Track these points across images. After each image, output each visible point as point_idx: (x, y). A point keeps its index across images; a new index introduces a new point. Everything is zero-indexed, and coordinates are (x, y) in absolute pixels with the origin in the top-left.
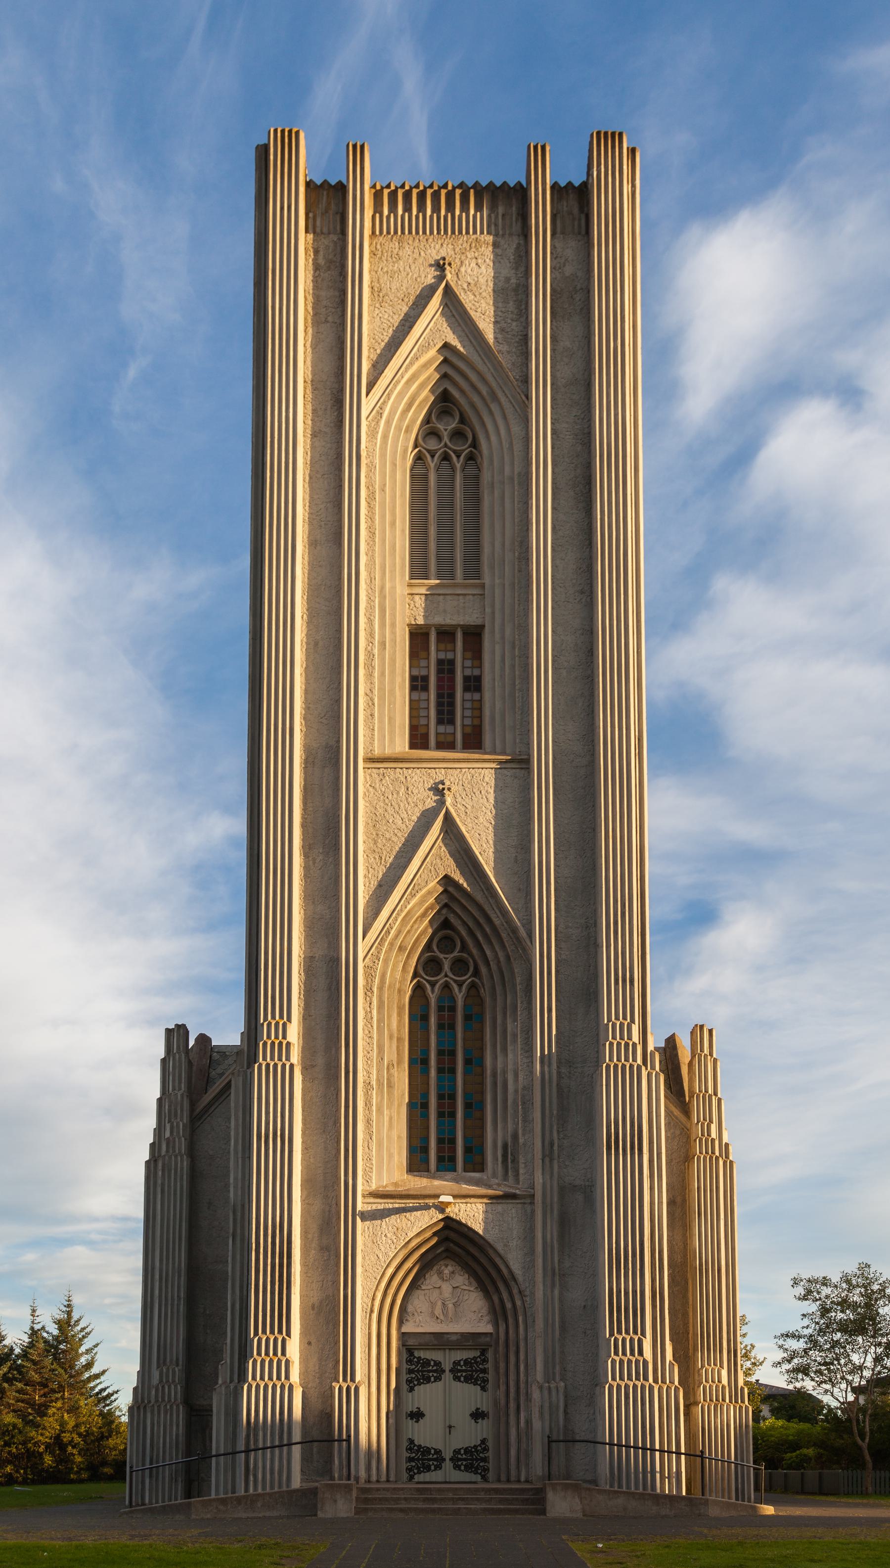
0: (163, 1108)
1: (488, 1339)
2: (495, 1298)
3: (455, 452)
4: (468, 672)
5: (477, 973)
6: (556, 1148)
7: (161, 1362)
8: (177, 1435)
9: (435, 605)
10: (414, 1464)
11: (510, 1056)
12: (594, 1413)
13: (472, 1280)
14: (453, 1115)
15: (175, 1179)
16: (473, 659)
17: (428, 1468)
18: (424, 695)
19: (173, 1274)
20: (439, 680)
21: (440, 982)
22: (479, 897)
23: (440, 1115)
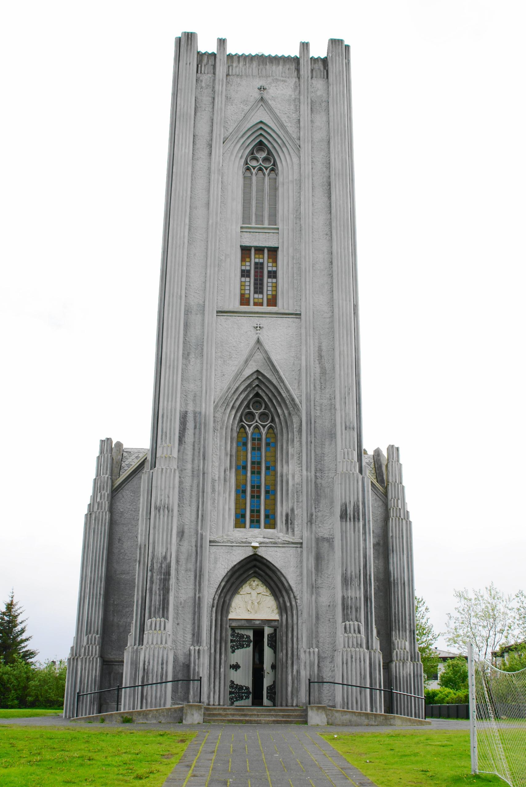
0: (97, 485)
1: (276, 623)
2: (281, 600)
3: (265, 167)
4: (270, 269)
5: (273, 421)
6: (314, 517)
7: (88, 631)
8: (96, 676)
9: (254, 237)
10: (234, 695)
11: (290, 466)
12: (334, 667)
13: (268, 589)
14: (259, 497)
15: (102, 525)
16: (273, 262)
17: (242, 698)
18: (248, 279)
19: (98, 580)
20: (256, 272)
21: (254, 425)
22: (275, 382)
23: (252, 497)
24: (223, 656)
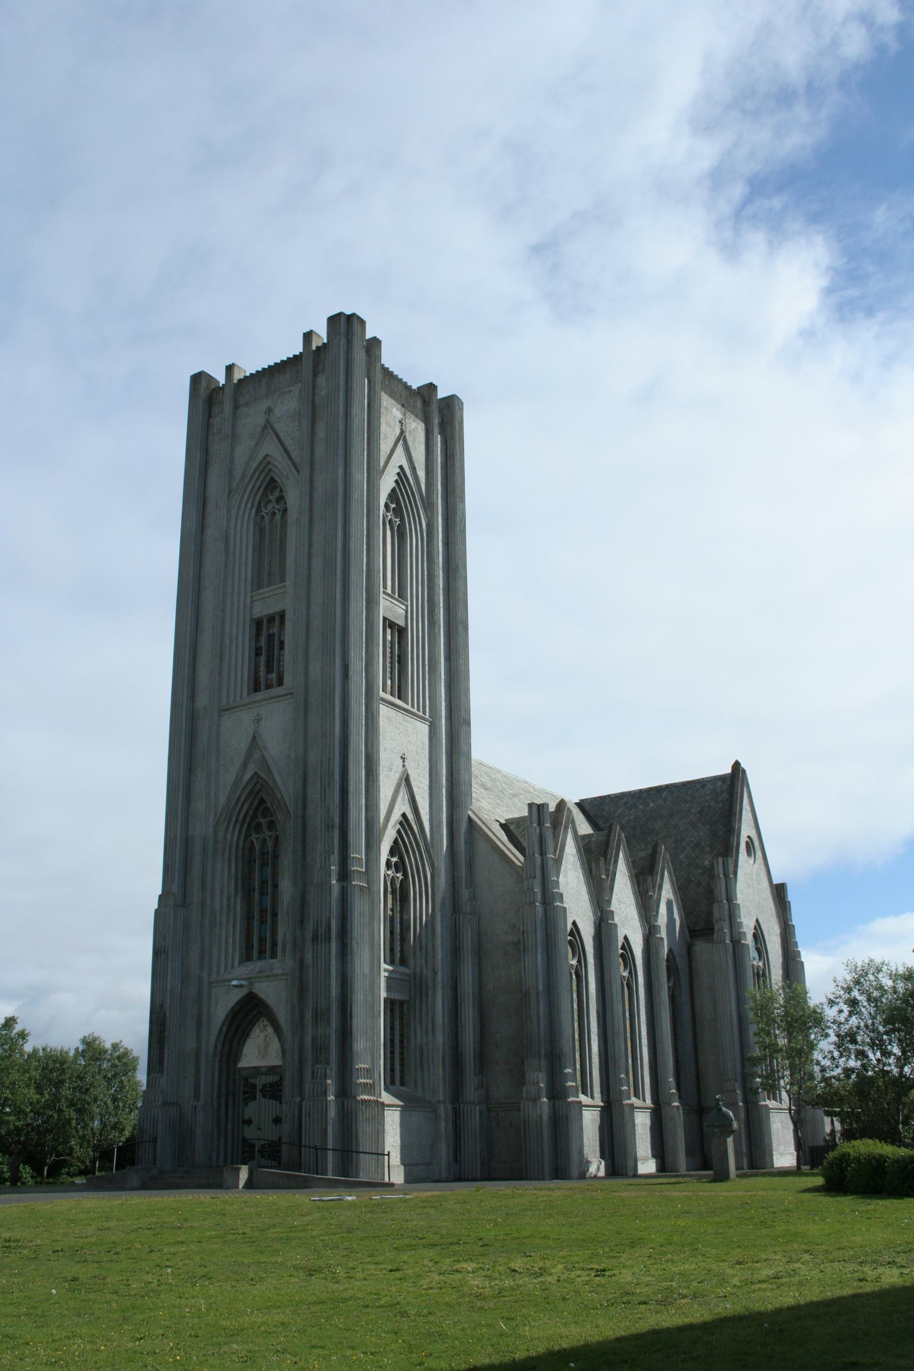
24: (230, 1112)
